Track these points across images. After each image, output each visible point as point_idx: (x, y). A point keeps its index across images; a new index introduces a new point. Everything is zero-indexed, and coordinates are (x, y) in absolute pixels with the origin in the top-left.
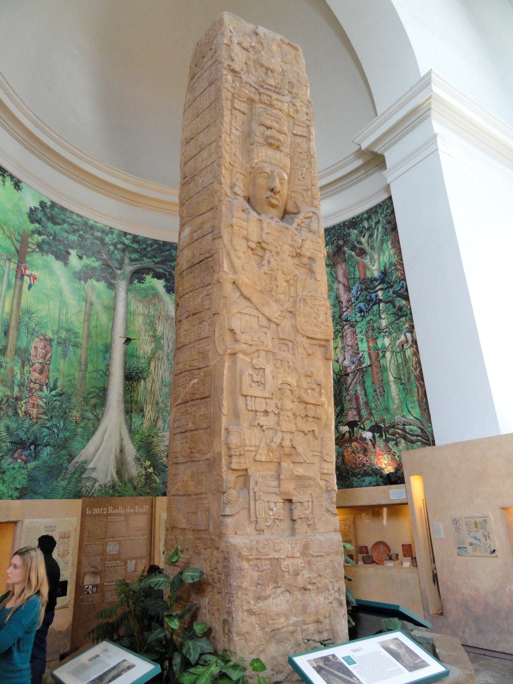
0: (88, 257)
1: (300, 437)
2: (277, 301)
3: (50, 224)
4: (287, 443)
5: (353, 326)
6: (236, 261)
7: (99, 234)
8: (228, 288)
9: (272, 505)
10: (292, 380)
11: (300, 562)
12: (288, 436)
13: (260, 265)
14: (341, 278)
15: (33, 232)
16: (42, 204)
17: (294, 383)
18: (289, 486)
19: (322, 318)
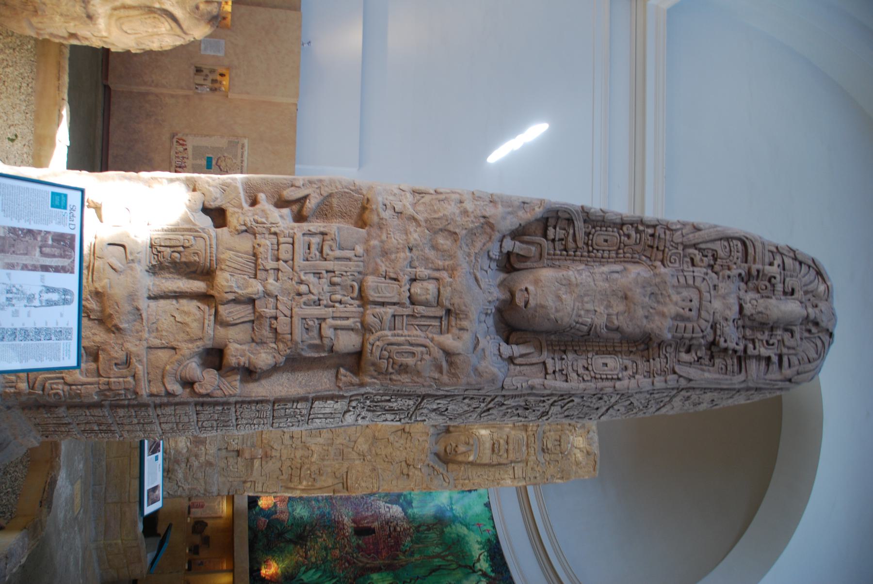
1: (278, 464)
2: (370, 450)
4: (274, 453)
9: (236, 441)
10: (315, 458)
11: (202, 459)
12: (278, 455)
17: (313, 460)
18: (247, 455)
19: (363, 484)
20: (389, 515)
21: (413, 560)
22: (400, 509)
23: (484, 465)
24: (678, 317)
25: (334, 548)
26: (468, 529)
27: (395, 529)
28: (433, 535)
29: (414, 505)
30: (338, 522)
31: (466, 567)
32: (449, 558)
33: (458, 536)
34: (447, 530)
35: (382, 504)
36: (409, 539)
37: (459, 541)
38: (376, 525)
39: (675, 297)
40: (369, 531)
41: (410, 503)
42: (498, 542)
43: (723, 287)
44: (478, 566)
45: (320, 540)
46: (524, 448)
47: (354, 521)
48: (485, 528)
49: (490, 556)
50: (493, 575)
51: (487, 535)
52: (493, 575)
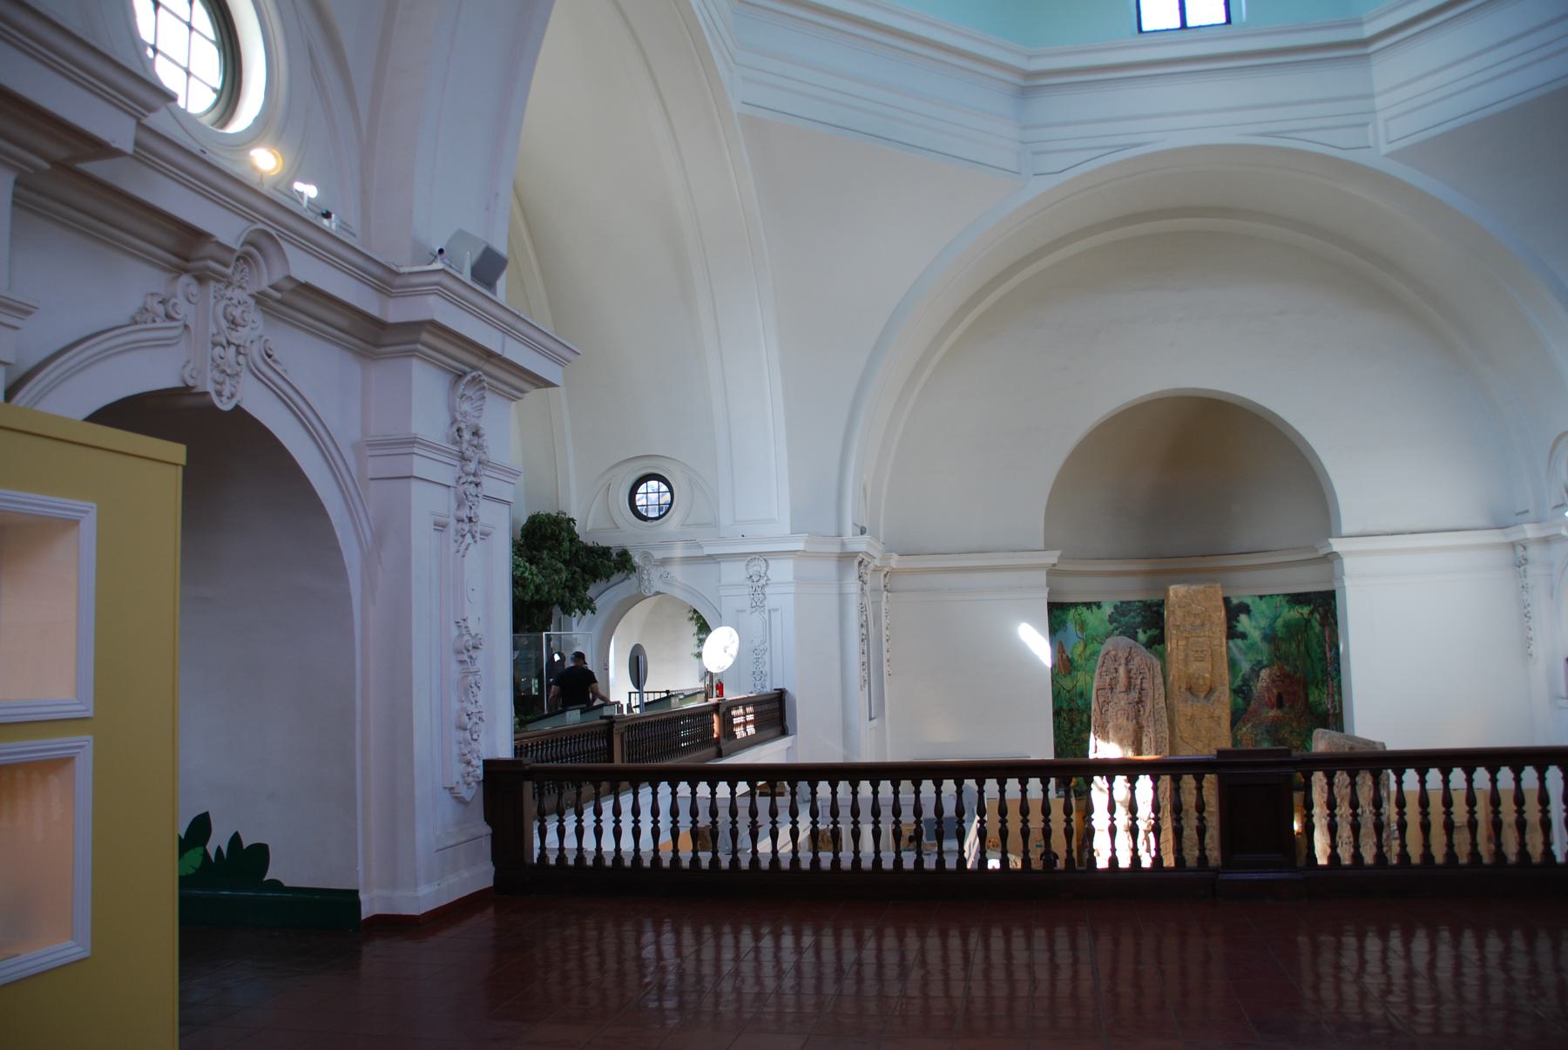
0: (1150, 629)
2: (1201, 741)
3: (1122, 619)
5: (1332, 680)
6: (1182, 728)
7: (1155, 609)
8: (1178, 739)
13: (1192, 726)
14: (1327, 638)
15: (1113, 630)
16: (1116, 607)
20: (1268, 680)
21: (1300, 667)
22: (1264, 671)
23: (1212, 665)
24: (1128, 719)
25: (1291, 726)
26: (1279, 616)
27: (1278, 676)
28: (1283, 647)
29: (1260, 658)
30: (1273, 720)
31: (1306, 626)
32: (1300, 637)
33: (1284, 626)
34: (1280, 635)
35: (1259, 684)
36: (1285, 667)
37: (1288, 625)
38: (1275, 691)
39: (1120, 721)
40: (1279, 697)
41: (1259, 662)
42: (1289, 595)
43: (1116, 700)
44: (1306, 616)
45: (1286, 735)
46: (1200, 639)
47: (1272, 708)
48: (1278, 602)
49: (1298, 604)
50: (1312, 606)
51: (1284, 603)
52: (1312, 606)
